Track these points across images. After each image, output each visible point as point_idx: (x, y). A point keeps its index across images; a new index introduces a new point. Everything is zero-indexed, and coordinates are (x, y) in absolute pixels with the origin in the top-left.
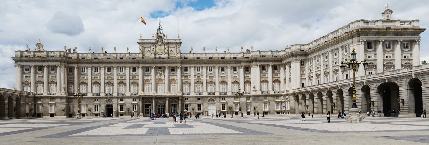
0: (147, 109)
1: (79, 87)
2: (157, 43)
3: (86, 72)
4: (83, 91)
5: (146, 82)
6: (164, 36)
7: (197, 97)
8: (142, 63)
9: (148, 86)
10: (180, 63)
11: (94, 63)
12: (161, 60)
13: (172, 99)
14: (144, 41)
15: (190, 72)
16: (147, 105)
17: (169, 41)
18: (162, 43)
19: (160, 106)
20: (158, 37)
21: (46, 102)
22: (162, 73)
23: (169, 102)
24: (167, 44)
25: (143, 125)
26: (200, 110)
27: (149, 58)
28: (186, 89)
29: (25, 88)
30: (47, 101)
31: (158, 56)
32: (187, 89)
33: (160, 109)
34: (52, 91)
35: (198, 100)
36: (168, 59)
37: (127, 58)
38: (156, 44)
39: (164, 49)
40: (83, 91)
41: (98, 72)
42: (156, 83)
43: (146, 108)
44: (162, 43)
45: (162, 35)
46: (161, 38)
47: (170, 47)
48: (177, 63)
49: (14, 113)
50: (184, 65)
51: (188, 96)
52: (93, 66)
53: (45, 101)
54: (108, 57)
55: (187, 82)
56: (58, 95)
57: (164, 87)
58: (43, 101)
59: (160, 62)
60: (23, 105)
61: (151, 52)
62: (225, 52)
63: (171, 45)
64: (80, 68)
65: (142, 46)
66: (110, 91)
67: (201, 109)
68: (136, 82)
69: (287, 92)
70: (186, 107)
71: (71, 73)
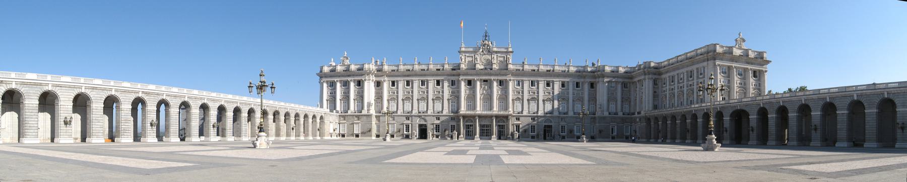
0: (468, 131)
4: (392, 108)
9: (471, 102)
16: (468, 125)
23: (496, 122)
25: (468, 150)
26: (534, 132)
28: (517, 107)
40: (392, 108)
55: (519, 98)
62: (566, 64)
67: (536, 132)
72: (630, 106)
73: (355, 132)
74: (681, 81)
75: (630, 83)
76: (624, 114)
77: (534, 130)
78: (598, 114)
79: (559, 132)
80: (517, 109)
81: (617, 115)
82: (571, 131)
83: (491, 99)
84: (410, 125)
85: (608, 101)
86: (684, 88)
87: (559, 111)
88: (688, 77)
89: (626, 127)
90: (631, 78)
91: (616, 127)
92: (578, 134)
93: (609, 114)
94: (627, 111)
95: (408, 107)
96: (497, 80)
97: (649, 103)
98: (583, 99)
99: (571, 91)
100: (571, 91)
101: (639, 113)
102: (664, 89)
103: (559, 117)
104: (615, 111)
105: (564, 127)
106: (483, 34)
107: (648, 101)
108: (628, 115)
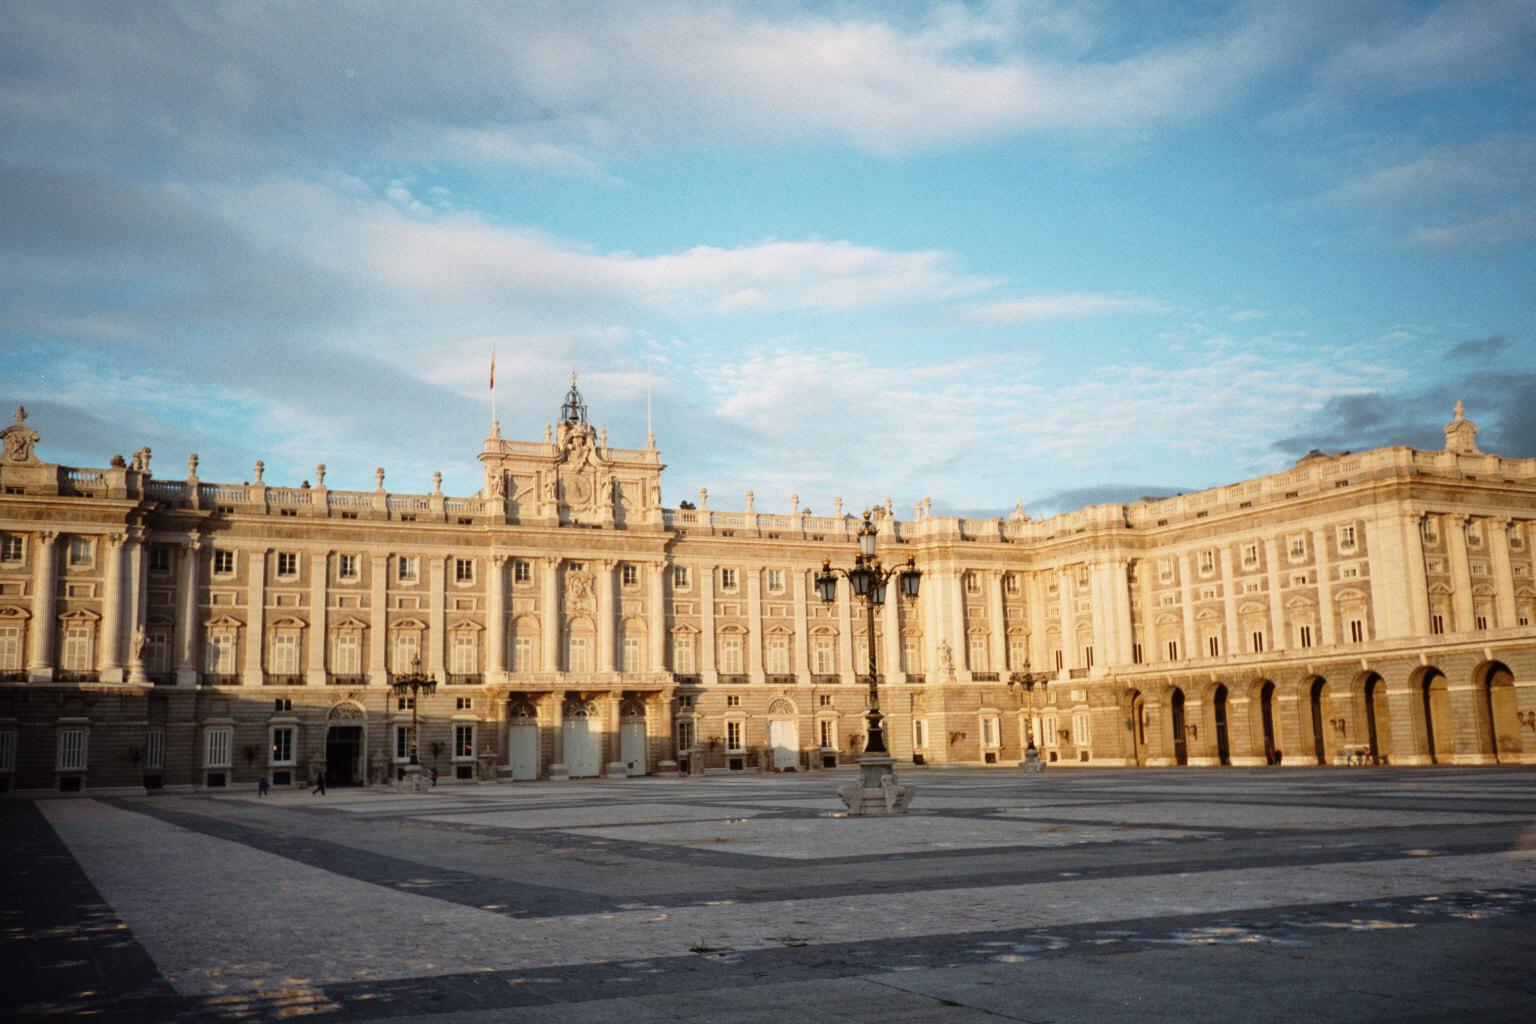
2: (565, 460)
3: (238, 573)
8: (504, 544)
10: (662, 548)
15: (699, 589)
17: (616, 457)
18: (584, 464)
20: (573, 438)
24: (606, 469)
27: (530, 521)
28: (681, 658)
32: (688, 655)
34: (71, 659)
35: (730, 703)
36: (619, 533)
41: (296, 577)
56: (111, 677)
57: (596, 646)
59: (583, 544)
61: (539, 496)
65: (502, 469)
69: (1072, 677)
71: (164, 576)
73: (61, 767)
74: (1245, 568)
80: (681, 665)
84: (296, 731)
86: (1265, 585)
88: (1283, 555)
93: (975, 677)
97: (1117, 639)
102: (1172, 593)
103: (813, 691)
107: (1116, 632)
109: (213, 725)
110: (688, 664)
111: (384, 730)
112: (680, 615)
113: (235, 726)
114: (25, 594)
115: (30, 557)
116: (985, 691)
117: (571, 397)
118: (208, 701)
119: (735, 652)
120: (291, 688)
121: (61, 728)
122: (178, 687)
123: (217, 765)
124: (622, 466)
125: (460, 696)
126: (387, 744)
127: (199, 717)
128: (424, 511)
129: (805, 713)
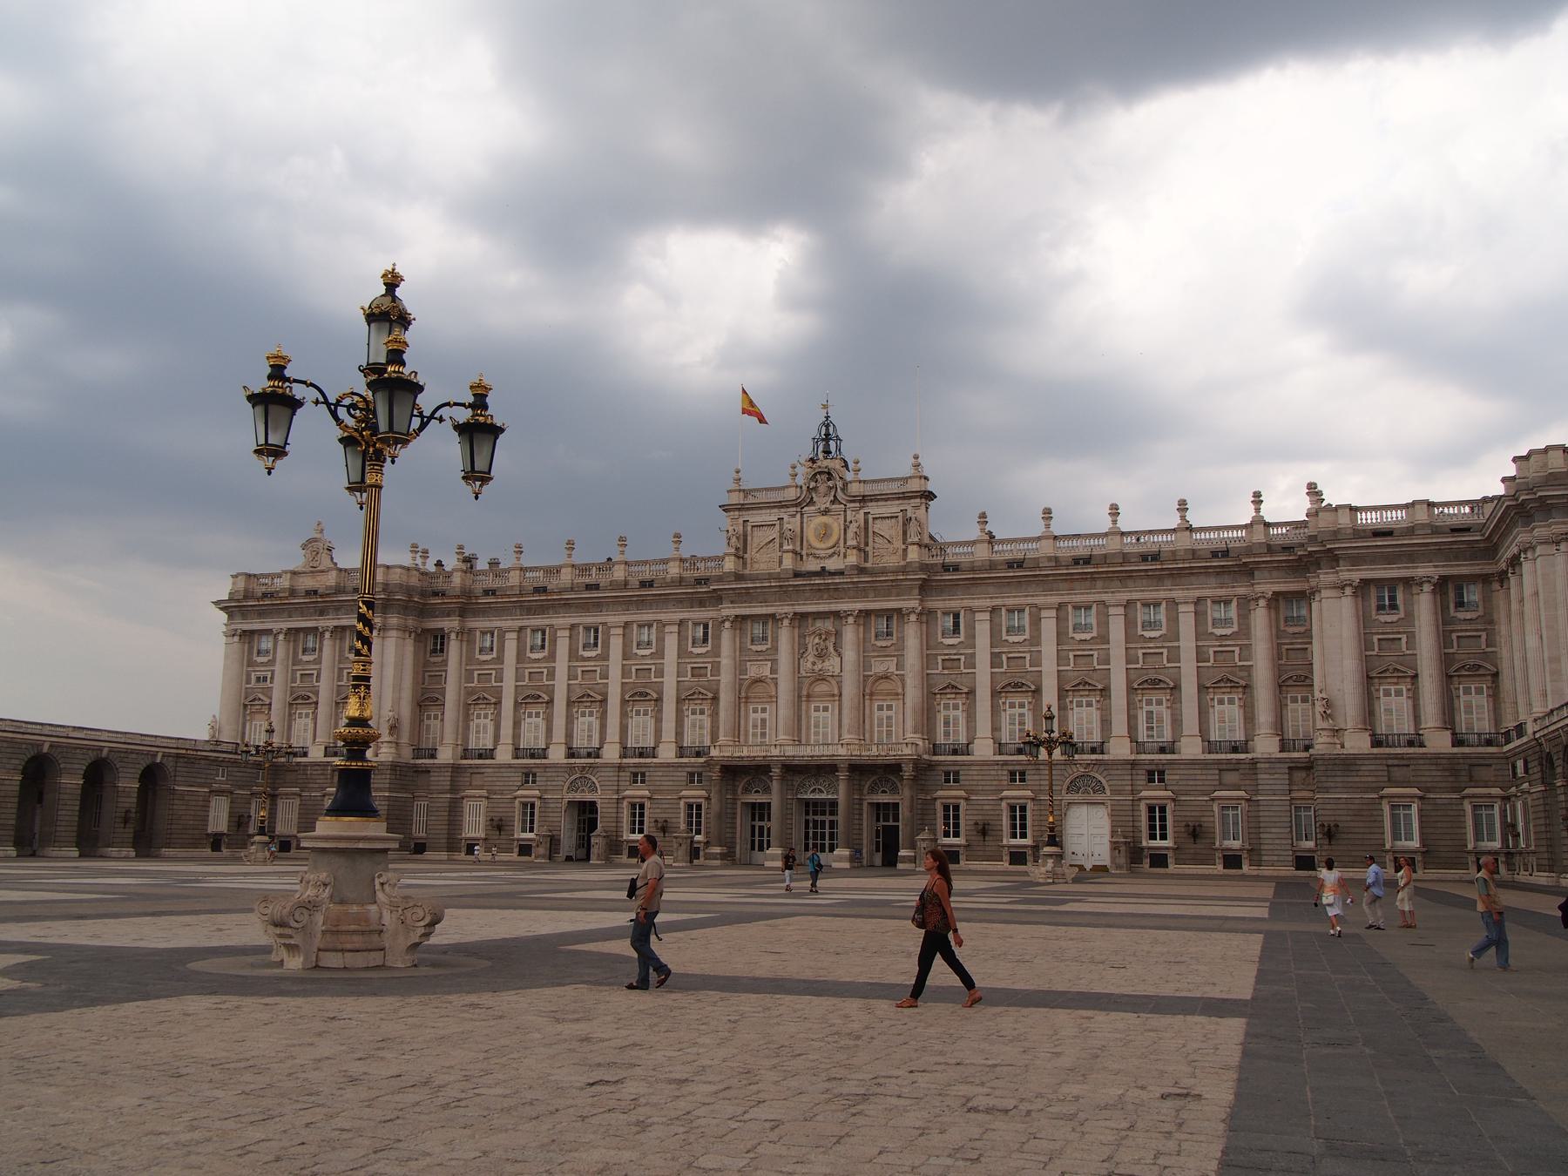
0: (761, 828)
1: (467, 718)
2: (811, 502)
4: (478, 738)
5: (749, 691)
6: (846, 466)
7: (1006, 763)
8: (732, 602)
9: (764, 710)
10: (916, 591)
11: (530, 610)
12: (824, 582)
13: (875, 778)
14: (750, 500)
17: (868, 490)
18: (833, 502)
19: (823, 813)
20: (815, 475)
21: (317, 786)
22: (831, 649)
24: (858, 505)
27: (769, 573)
28: (947, 723)
29: (251, 729)
30: (318, 781)
31: (812, 565)
32: (956, 719)
33: (823, 822)
37: (668, 580)
38: (805, 509)
39: (845, 530)
40: (478, 738)
42: (800, 697)
43: (753, 819)
44: (835, 501)
45: (837, 464)
46: (829, 479)
47: (874, 518)
48: (894, 588)
49: (128, 833)
50: (936, 603)
51: (955, 763)
52: (526, 623)
53: (311, 781)
54: (588, 580)
55: (954, 687)
58: (306, 781)
59: (819, 592)
60: (186, 798)
61: (781, 546)
63: (875, 509)
64: (475, 635)
65: (741, 520)
66: (590, 737)
67: (1029, 832)
68: (705, 692)
70: (946, 817)
71: (440, 659)
72: (1495, 696)
75: (1485, 579)
76: (1458, 742)
77: (1023, 826)
78: (1322, 745)
79: (1136, 829)
81: (1422, 745)
82: (1195, 832)
83: (840, 695)
84: (538, 804)
85: (1368, 676)
87: (1133, 739)
89: (1475, 807)
90: (1489, 549)
91: (1415, 807)
92: (1236, 844)
93: (1376, 743)
94: (1484, 724)
95: (532, 734)
96: (866, 614)
98: (1249, 675)
99: (1187, 643)
100: (1187, 643)
101: (1520, 730)
103: (1134, 764)
104: (1407, 728)
105: (1163, 809)
106: (813, 429)
108: (1489, 743)
109: (467, 797)
110: (956, 732)
111: (615, 805)
112: (946, 672)
113: (488, 798)
114: (317, 682)
115: (321, 650)
116: (1396, 762)
117: (823, 432)
118: (469, 775)
119: (1021, 715)
120: (533, 761)
121: (327, 797)
122: (436, 761)
123: (472, 835)
124: (874, 498)
125: (689, 770)
126: (618, 821)
127: (454, 789)
128: (662, 575)
129: (1119, 792)
